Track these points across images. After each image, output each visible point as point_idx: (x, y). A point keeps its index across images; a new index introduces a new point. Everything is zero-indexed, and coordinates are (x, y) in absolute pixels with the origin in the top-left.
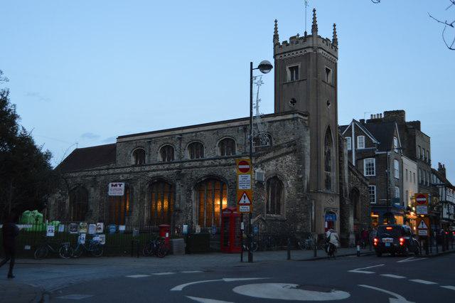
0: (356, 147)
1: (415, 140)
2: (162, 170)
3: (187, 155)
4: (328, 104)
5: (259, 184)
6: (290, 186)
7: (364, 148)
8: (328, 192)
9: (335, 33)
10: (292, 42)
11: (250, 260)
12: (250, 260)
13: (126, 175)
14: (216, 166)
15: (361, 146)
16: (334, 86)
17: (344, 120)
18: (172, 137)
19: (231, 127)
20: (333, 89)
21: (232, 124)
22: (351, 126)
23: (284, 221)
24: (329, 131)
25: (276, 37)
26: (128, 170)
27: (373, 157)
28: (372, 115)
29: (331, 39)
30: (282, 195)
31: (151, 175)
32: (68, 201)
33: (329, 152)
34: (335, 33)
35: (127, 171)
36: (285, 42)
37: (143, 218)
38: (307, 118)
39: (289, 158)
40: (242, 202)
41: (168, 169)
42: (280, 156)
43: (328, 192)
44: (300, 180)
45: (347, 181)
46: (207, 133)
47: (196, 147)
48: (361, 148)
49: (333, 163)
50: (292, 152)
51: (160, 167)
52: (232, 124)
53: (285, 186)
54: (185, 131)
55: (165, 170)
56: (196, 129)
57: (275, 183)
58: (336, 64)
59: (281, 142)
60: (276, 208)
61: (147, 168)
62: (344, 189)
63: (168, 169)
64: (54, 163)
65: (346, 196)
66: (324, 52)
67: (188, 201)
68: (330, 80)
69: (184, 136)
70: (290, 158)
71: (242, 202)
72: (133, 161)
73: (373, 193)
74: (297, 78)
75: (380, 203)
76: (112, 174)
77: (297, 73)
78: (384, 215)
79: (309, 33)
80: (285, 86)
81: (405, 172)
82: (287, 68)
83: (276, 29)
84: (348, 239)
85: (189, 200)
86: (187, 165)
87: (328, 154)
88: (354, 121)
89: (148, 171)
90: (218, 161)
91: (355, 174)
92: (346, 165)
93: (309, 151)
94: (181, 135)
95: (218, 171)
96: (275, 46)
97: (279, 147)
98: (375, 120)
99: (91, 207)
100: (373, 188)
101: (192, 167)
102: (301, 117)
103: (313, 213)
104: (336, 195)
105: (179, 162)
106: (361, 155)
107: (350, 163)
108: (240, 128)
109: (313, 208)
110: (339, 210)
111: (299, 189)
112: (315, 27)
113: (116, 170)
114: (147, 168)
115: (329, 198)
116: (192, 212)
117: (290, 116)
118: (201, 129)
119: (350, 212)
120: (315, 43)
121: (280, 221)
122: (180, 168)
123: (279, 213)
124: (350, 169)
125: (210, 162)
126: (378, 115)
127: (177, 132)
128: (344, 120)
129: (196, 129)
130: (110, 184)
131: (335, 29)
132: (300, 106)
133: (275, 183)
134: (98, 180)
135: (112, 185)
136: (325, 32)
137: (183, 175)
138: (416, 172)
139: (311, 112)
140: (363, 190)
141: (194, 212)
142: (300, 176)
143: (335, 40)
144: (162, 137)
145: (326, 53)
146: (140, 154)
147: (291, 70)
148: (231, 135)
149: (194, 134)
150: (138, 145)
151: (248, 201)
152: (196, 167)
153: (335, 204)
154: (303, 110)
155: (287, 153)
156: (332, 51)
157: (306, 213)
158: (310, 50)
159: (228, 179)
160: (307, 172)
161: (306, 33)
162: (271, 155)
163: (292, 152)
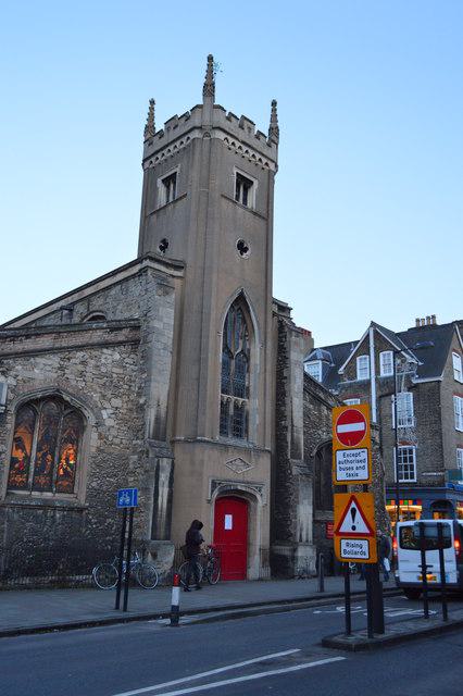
0: (378, 372)
6: (109, 422)
10: (168, 129)
16: (265, 216)
20: (263, 223)
23: (80, 510)
24: (240, 303)
25: (150, 128)
28: (418, 320)
29: (263, 126)
33: (246, 355)
39: (110, 357)
43: (231, 441)
44: (141, 408)
48: (388, 375)
50: (120, 343)
53: (92, 420)
58: (271, 175)
62: (289, 439)
65: (296, 455)
66: (231, 140)
70: (117, 356)
75: (424, 481)
78: (434, 505)
84: (294, 558)
87: (237, 364)
88: (373, 324)
98: (424, 327)
102: (156, 266)
103: (164, 491)
104: (260, 451)
106: (388, 388)
109: (164, 477)
110: (266, 490)
111: (138, 431)
112: (209, 89)
115: (232, 455)
119: (301, 494)
121: (64, 509)
126: (428, 318)
132: (174, 253)
139: (189, 261)
142: (142, 401)
143: (274, 130)
145: (238, 144)
147: (168, 187)
153: (256, 474)
155: (106, 345)
157: (146, 490)
160: (160, 389)
163: (120, 343)
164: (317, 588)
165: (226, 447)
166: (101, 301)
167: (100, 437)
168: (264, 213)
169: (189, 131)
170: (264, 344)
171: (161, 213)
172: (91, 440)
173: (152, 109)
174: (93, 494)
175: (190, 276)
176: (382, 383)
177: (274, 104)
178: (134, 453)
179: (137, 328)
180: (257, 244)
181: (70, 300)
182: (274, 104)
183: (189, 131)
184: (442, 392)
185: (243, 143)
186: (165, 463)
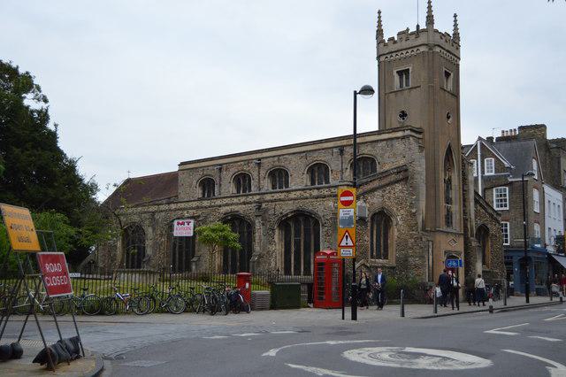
0: (483, 172)
1: (559, 163)
2: (237, 204)
3: (267, 184)
4: (448, 118)
5: (361, 220)
7: (493, 174)
8: (449, 230)
9: (456, 25)
11: (354, 317)
12: (354, 317)
13: (190, 211)
14: (307, 198)
15: (490, 173)
17: (468, 137)
18: (248, 162)
19: (323, 149)
20: (454, 99)
21: (325, 145)
22: (476, 146)
23: (393, 268)
24: (449, 151)
25: (380, 32)
26: (194, 204)
27: (505, 185)
28: (503, 132)
29: (451, 33)
30: (390, 233)
31: (223, 210)
32: (119, 244)
33: (450, 180)
34: (456, 25)
36: (391, 39)
38: (420, 136)
39: (399, 187)
40: (343, 244)
41: (244, 203)
42: (388, 185)
44: (414, 214)
45: (473, 217)
46: (290, 157)
47: (279, 176)
49: (455, 194)
51: (235, 200)
52: (325, 145)
53: (395, 223)
54: (265, 155)
56: (279, 153)
57: (381, 219)
58: (458, 65)
59: (387, 168)
60: (382, 251)
61: (218, 202)
62: (469, 227)
63: (244, 203)
64: (101, 197)
68: (450, 87)
71: (343, 244)
72: (199, 192)
73: (506, 231)
74: (407, 84)
76: (176, 210)
77: (407, 78)
79: (423, 26)
80: (392, 96)
81: (546, 204)
82: (395, 72)
83: (379, 22)
86: (268, 197)
87: (448, 182)
88: (480, 138)
89: (220, 206)
90: (308, 191)
91: (484, 208)
92: (472, 195)
93: (423, 177)
95: (309, 206)
96: (378, 44)
97: (386, 174)
99: (149, 251)
100: (506, 225)
101: (276, 200)
103: (431, 257)
105: (259, 194)
106: (490, 183)
107: (476, 193)
108: (335, 150)
110: (463, 254)
111: (411, 227)
112: (430, 20)
113: (179, 205)
114: (218, 202)
117: (400, 134)
120: (431, 38)
121: (388, 268)
122: (259, 203)
123: (386, 257)
124: (476, 202)
125: (298, 193)
128: (468, 137)
129: (279, 153)
130: (176, 222)
131: (455, 21)
132: (410, 121)
133: (381, 219)
134: (157, 216)
135: (178, 224)
136: (443, 25)
137: (266, 210)
138: (561, 204)
140: (493, 229)
142: (414, 211)
143: (456, 35)
146: (208, 185)
149: (276, 159)
151: (351, 244)
152: (280, 200)
153: (459, 246)
154: (417, 125)
156: (452, 49)
157: (422, 257)
158: (422, 49)
159: (321, 214)
160: (423, 204)
161: (418, 26)
162: (376, 184)
164: (503, 304)
165: (448, 233)
166: (369, 148)
167: (398, 231)
168: (455, 93)
169: (420, 45)
170: (459, 176)
171: (399, 94)
172: (395, 233)
173: (379, 17)
174: (398, 259)
175: (427, 137)
176: (485, 179)
177: (455, 16)
178: (411, 238)
179: (406, 170)
180: (453, 114)
181: (339, 143)
182: (455, 16)
183: (420, 45)
184: (529, 187)
185: (448, 51)
186: (431, 244)
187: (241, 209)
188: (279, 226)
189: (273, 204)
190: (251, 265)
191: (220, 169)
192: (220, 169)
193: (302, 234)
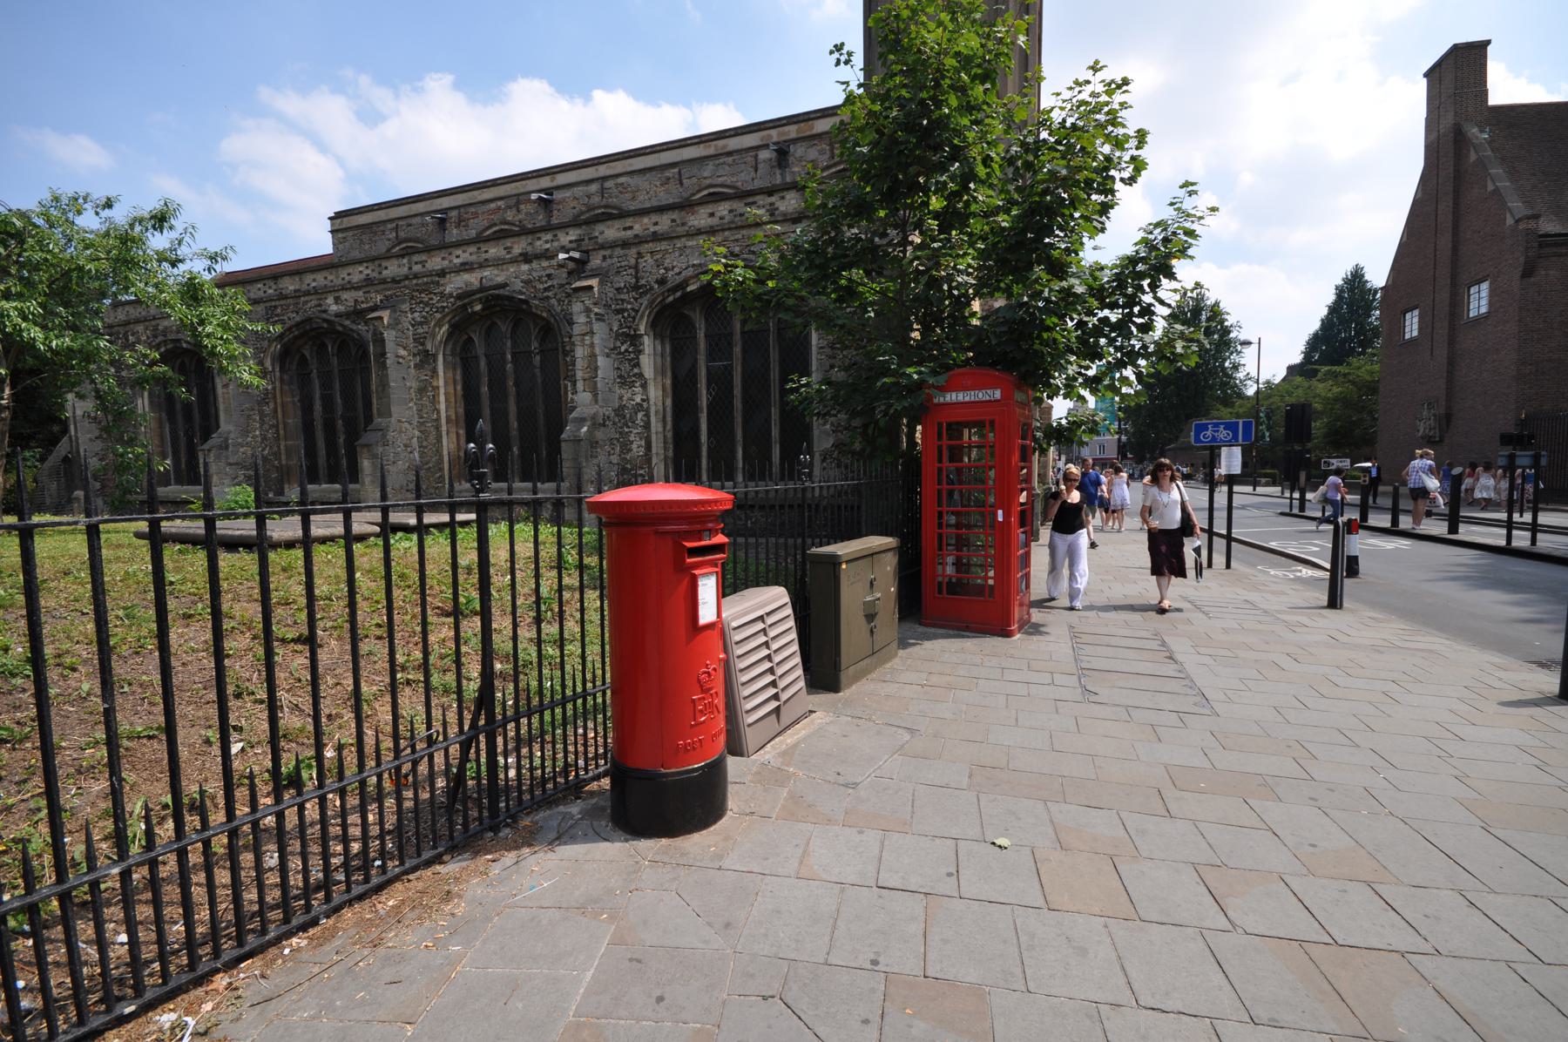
2: (499, 263)
13: (345, 295)
14: (757, 225)
18: (518, 200)
19: (729, 154)
31: (454, 284)
35: (356, 278)
37: (439, 452)
55: (514, 261)
56: (603, 170)
63: (526, 258)
67: (624, 381)
69: (557, 196)
76: (298, 294)
85: (629, 376)
89: (442, 273)
90: (762, 200)
94: (548, 191)
101: (639, 241)
108: (764, 155)
116: (647, 426)
118: (619, 167)
125: (723, 209)
127: (531, 185)
141: (655, 425)
144: (484, 202)
148: (729, 183)
149: (594, 188)
150: (402, 234)
152: (656, 237)
181: (774, 135)
187: (514, 277)
188: (654, 325)
189: (634, 251)
190: (566, 451)
191: (442, 221)
192: (442, 221)
193: (737, 350)
